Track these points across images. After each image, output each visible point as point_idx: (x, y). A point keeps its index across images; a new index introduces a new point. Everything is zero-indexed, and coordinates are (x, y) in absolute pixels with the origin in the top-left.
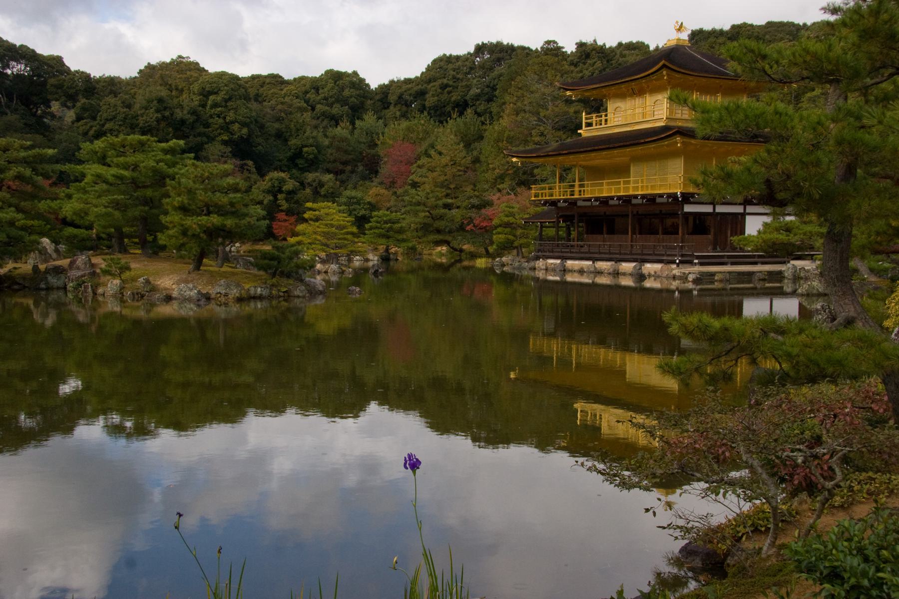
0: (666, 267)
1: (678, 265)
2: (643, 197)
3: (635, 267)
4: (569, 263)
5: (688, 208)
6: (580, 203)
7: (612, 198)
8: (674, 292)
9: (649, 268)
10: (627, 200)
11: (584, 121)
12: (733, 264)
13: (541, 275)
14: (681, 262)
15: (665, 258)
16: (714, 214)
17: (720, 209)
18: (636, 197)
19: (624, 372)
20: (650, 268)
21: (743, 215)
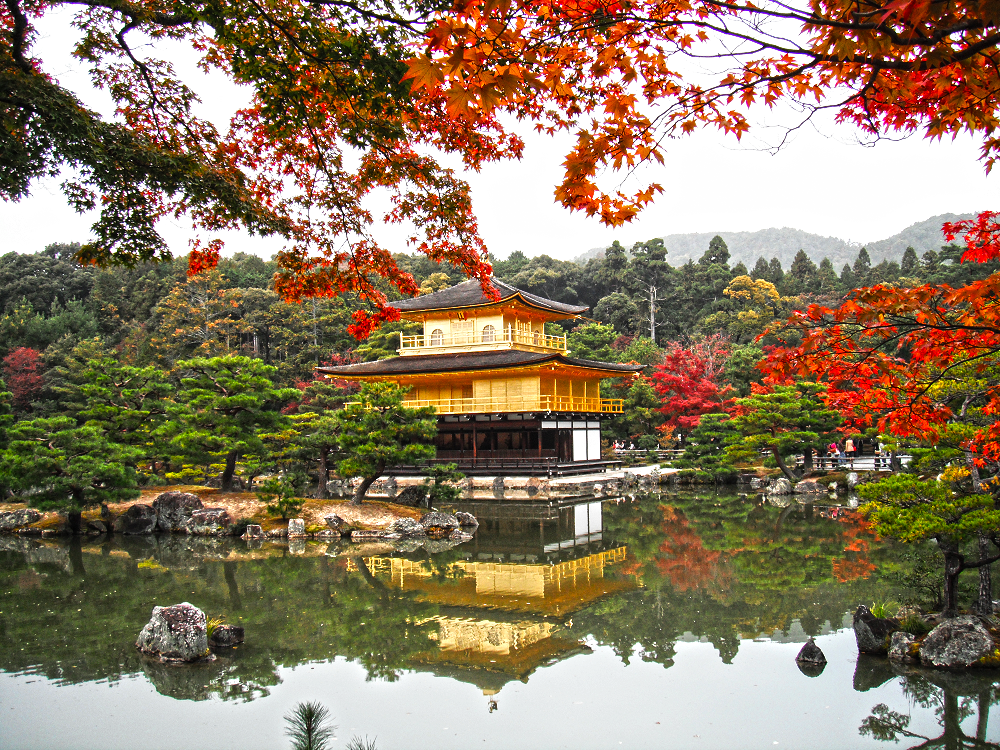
0: (534, 479)
2: (501, 414)
3: (496, 481)
5: (545, 425)
9: (509, 481)
10: (472, 417)
11: (402, 341)
12: (580, 473)
15: (533, 471)
16: (557, 430)
17: (563, 425)
19: (472, 583)
21: (572, 429)
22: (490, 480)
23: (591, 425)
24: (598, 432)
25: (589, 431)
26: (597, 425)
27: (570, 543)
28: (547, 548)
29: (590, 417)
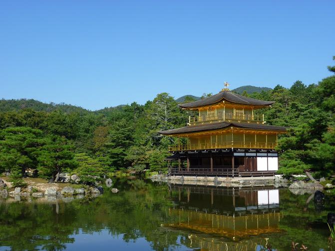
1: (233, 177)
4: (186, 177)
5: (235, 154)
6: (189, 152)
7: (204, 150)
8: (231, 188)
12: (254, 176)
13: (172, 182)
14: (235, 176)
17: (247, 154)
18: (214, 150)
20: (220, 179)
21: (256, 156)
22: (212, 178)
23: (269, 154)
24: (277, 158)
25: (269, 158)
26: (276, 155)
27: (255, 208)
28: (236, 209)
29: (268, 151)
